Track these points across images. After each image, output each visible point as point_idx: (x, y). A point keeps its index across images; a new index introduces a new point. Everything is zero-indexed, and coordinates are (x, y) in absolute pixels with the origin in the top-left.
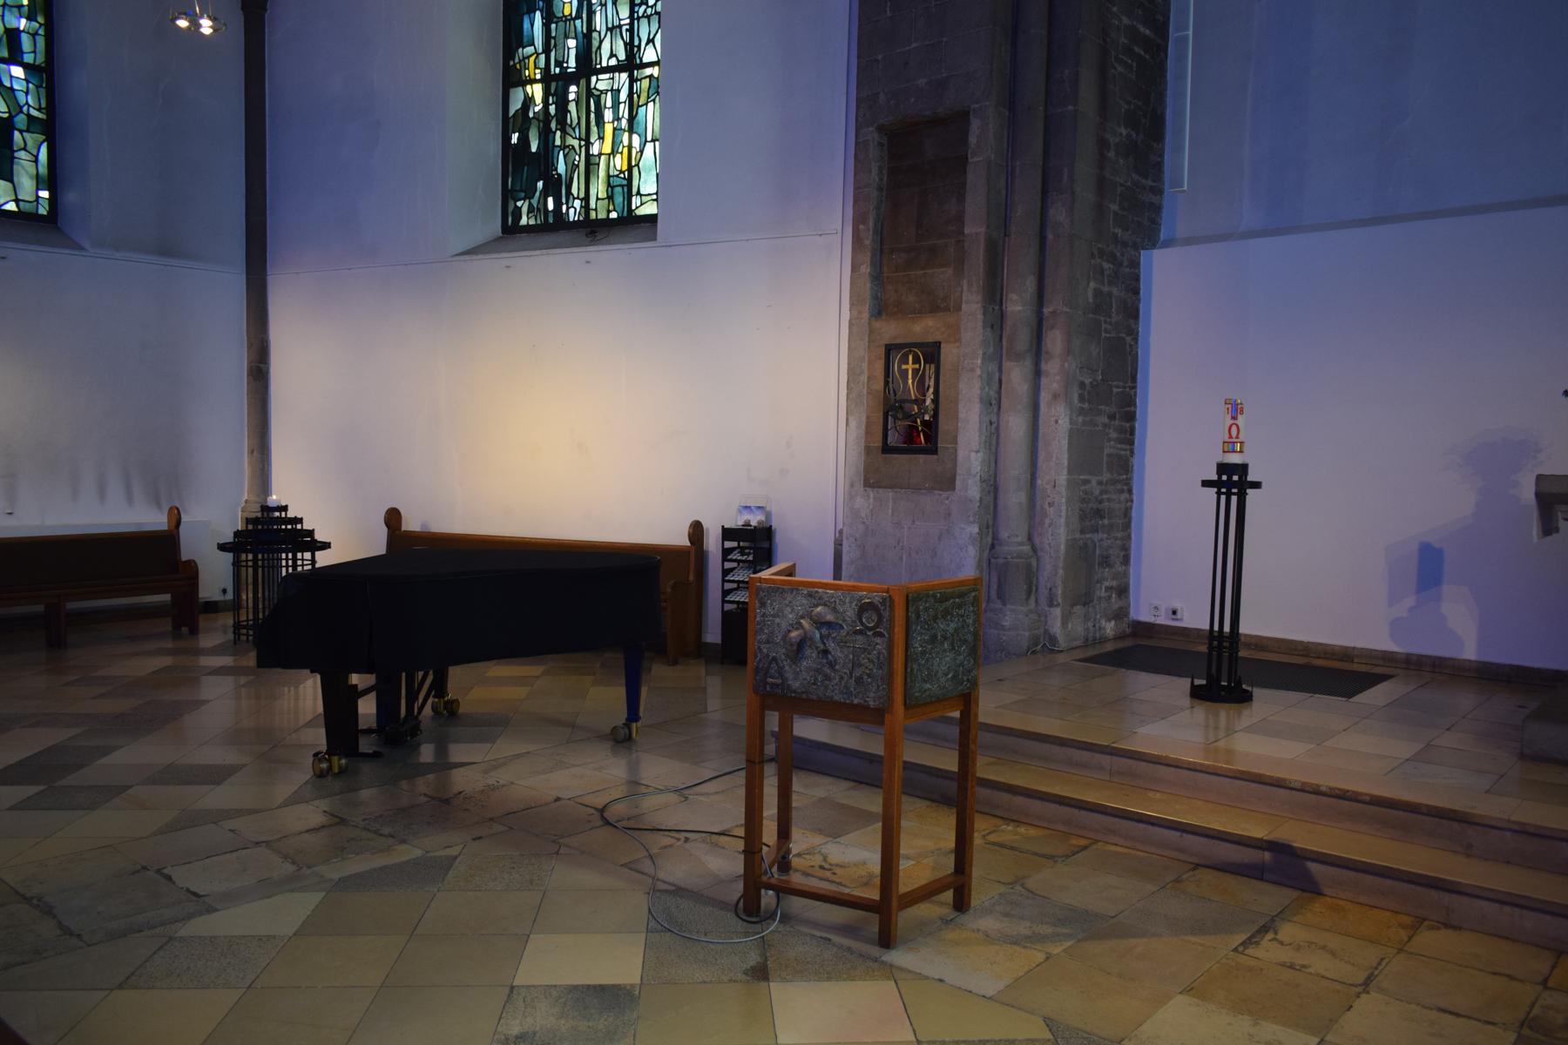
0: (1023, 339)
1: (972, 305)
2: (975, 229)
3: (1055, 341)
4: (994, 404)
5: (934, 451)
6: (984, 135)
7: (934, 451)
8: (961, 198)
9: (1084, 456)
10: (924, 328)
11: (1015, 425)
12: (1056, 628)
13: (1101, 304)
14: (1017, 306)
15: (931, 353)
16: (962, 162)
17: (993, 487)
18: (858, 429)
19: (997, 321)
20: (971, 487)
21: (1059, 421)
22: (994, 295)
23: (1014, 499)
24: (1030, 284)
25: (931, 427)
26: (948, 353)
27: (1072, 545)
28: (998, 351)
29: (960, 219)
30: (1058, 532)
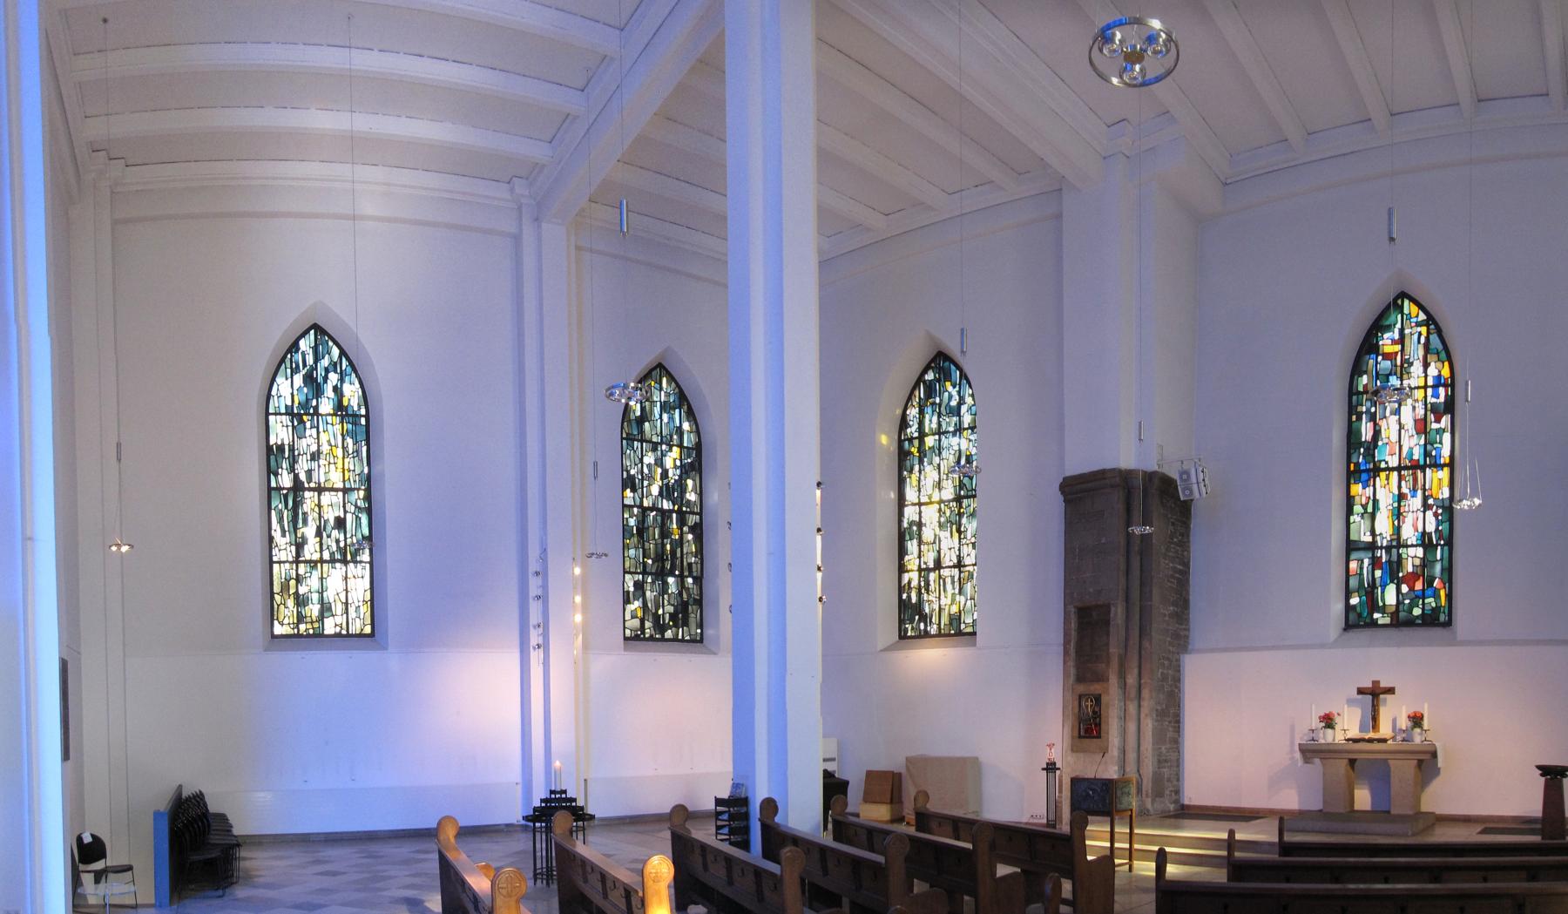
0: (1133, 693)
1: (1113, 680)
2: (1114, 650)
3: (1146, 693)
4: (1124, 718)
5: (1099, 736)
6: (1118, 613)
7: (1099, 736)
8: (1108, 634)
9: (1159, 737)
10: (1095, 688)
11: (1132, 727)
12: (1149, 806)
13: (1164, 678)
14: (1131, 680)
15: (1098, 699)
16: (1107, 623)
17: (1123, 752)
18: (1068, 730)
19: (1124, 686)
20: (1114, 752)
21: (1148, 725)
22: (1122, 676)
23: (1131, 756)
24: (1136, 671)
25: (1098, 725)
26: (1104, 699)
27: (1155, 773)
28: (1125, 697)
29: (1107, 645)
30: (1149, 768)
